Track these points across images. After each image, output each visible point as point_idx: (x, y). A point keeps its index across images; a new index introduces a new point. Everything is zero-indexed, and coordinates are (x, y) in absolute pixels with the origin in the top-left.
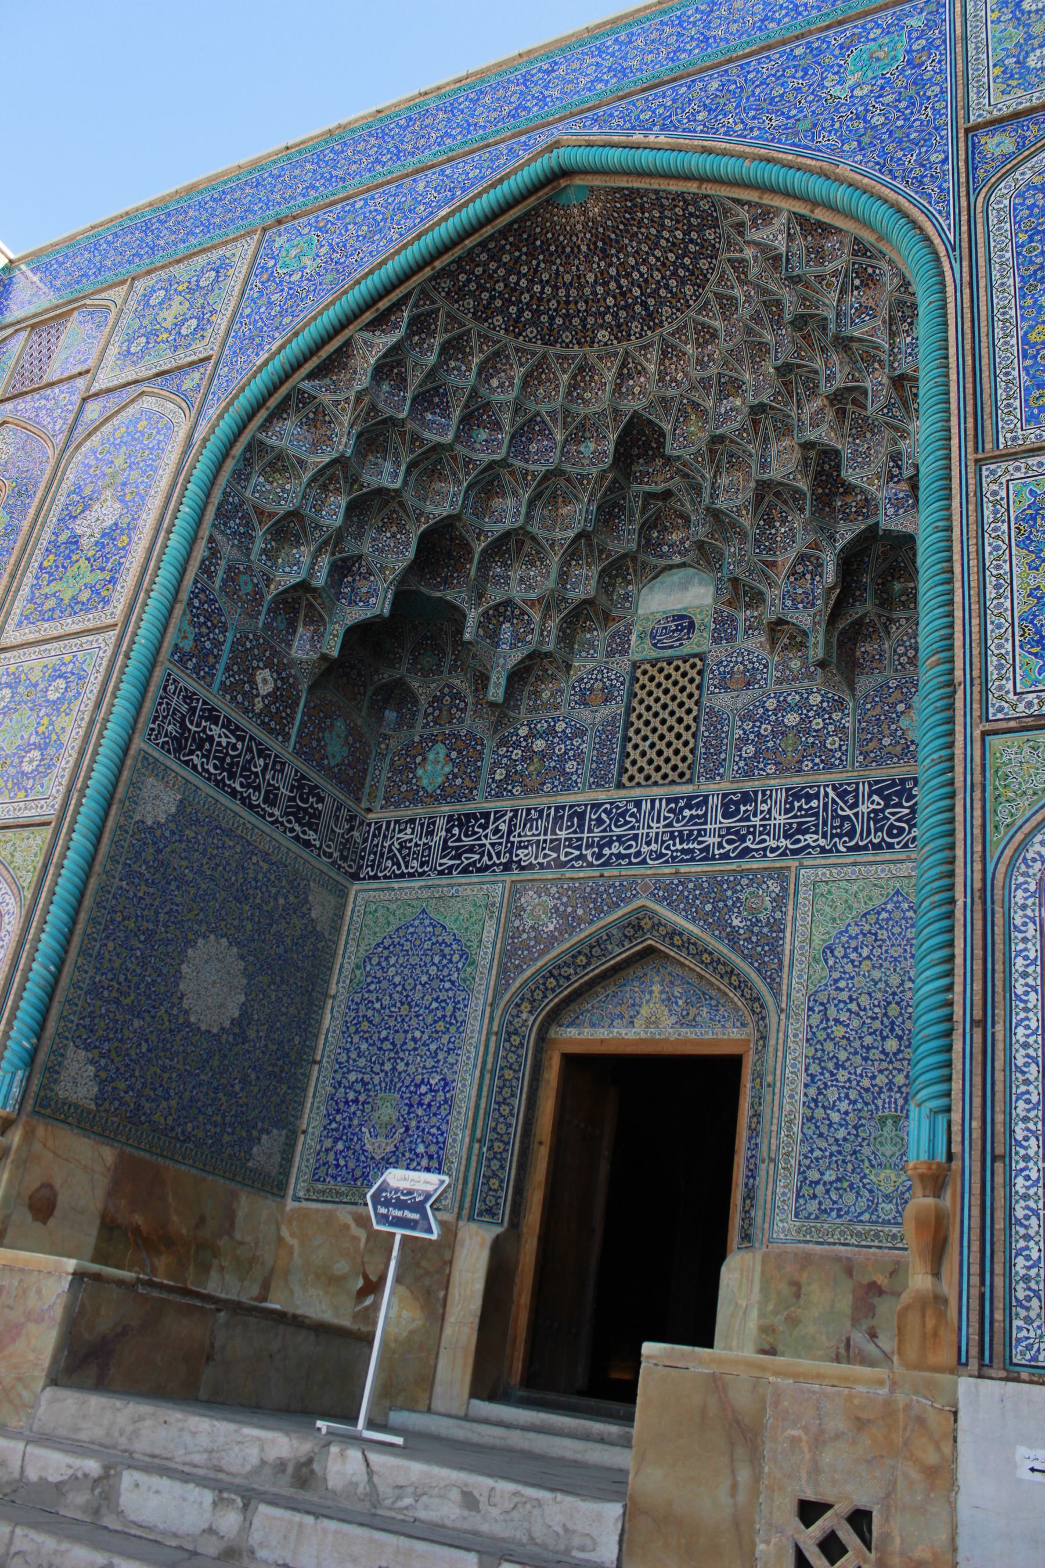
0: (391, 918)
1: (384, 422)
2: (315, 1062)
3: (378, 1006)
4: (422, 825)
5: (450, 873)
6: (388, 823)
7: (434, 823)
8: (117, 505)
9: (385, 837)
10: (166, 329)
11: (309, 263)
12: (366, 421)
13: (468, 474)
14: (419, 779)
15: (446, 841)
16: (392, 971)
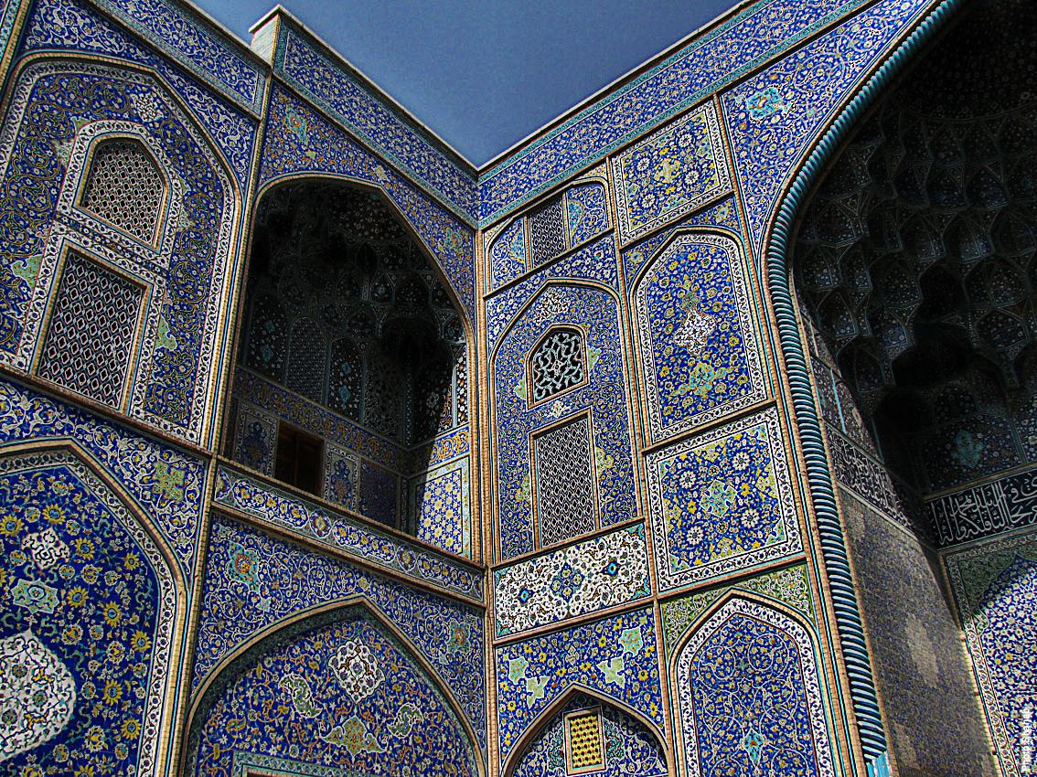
0: (988, 569)
1: (881, 206)
2: (976, 694)
3: (1013, 638)
4: (980, 494)
5: (1027, 523)
6: (946, 500)
7: (990, 490)
8: (708, 317)
9: (949, 511)
10: (669, 185)
11: (782, 107)
12: (870, 208)
13: (942, 227)
14: (957, 460)
15: (1009, 500)
16: (1012, 609)
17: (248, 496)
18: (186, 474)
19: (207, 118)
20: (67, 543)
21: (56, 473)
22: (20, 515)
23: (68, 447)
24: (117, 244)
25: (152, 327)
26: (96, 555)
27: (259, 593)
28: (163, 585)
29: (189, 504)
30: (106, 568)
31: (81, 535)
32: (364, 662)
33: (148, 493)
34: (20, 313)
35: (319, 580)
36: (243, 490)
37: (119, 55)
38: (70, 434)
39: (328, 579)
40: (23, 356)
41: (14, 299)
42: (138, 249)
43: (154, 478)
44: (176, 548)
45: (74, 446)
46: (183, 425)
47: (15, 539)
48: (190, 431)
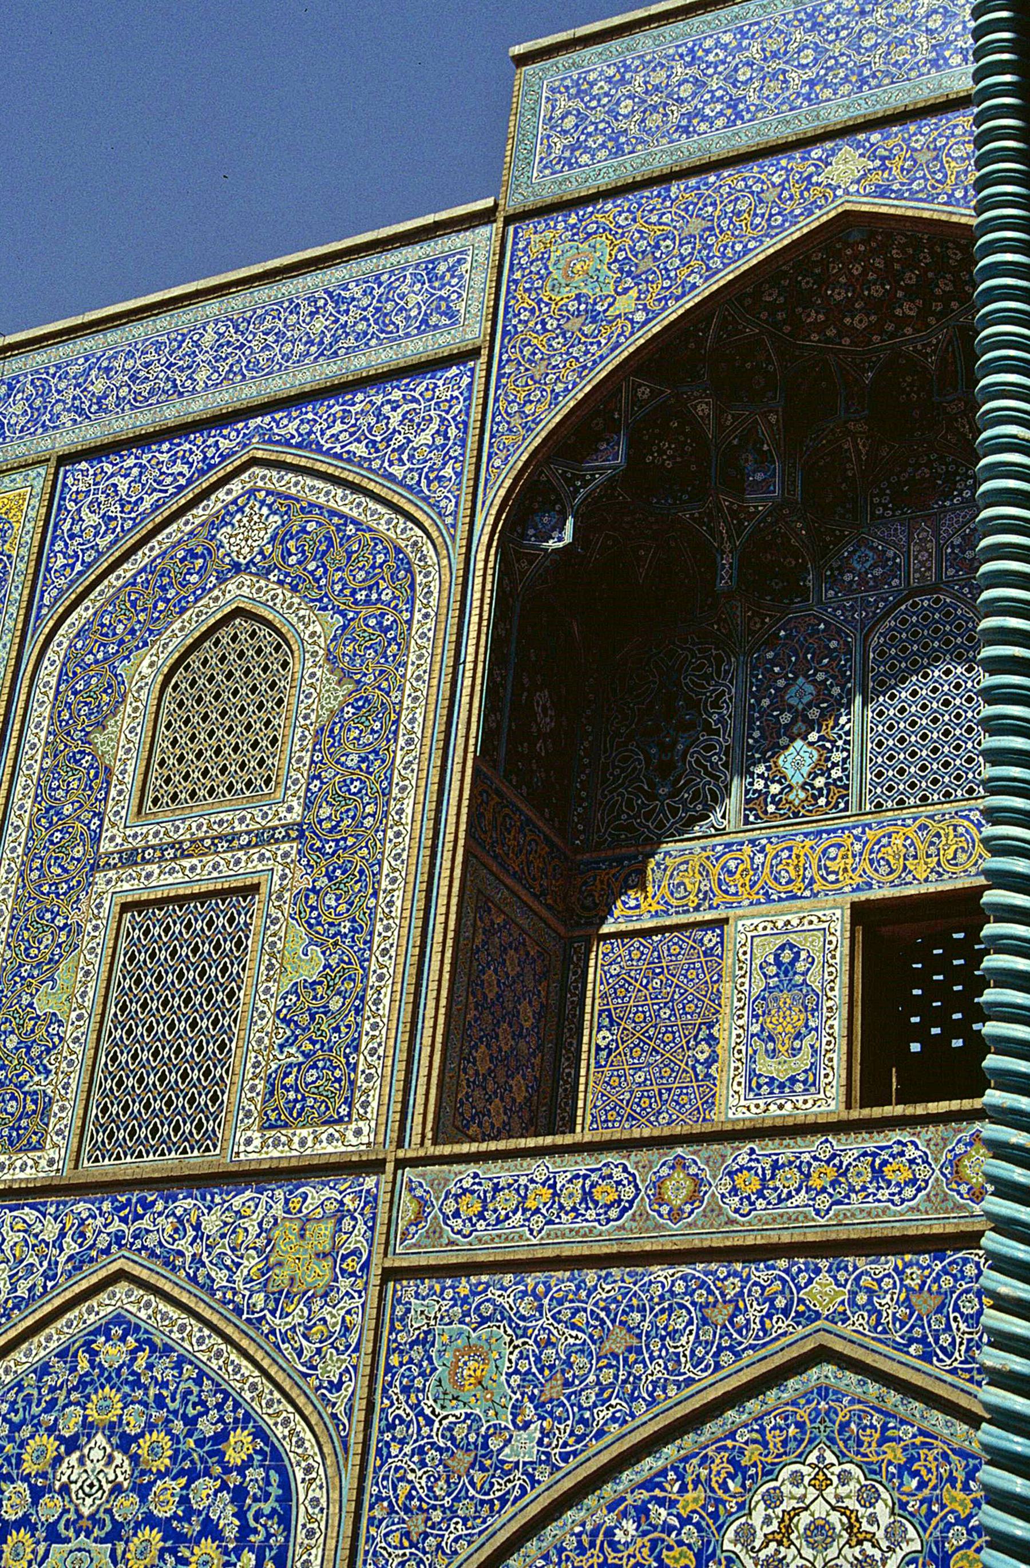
17: (478, 1207)
18: (340, 1221)
19: (360, 450)
20: (125, 1450)
21: (103, 1330)
22: (51, 1430)
23: (121, 1275)
24: (202, 840)
25: (273, 955)
26: (173, 1458)
27: (506, 1421)
28: (300, 1475)
29: (344, 1284)
30: (193, 1475)
31: (150, 1427)
32: (843, 1511)
33: (259, 1299)
34: (48, 1072)
35: (674, 1334)
36: (467, 1198)
37: (190, 481)
38: (121, 1246)
39: (705, 1321)
40: (56, 1145)
41: (39, 1057)
42: (242, 820)
43: (272, 1260)
44: (318, 1389)
45: (129, 1267)
46: (340, 1120)
47: (44, 1475)
48: (353, 1126)
